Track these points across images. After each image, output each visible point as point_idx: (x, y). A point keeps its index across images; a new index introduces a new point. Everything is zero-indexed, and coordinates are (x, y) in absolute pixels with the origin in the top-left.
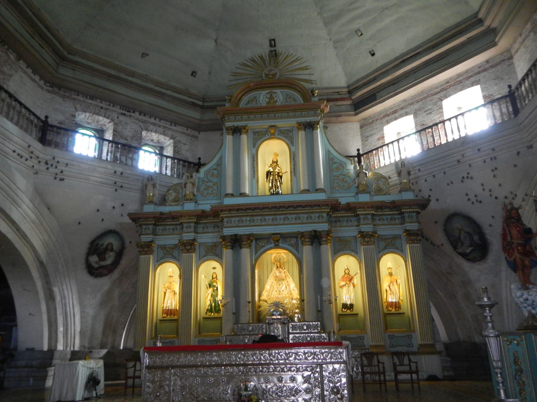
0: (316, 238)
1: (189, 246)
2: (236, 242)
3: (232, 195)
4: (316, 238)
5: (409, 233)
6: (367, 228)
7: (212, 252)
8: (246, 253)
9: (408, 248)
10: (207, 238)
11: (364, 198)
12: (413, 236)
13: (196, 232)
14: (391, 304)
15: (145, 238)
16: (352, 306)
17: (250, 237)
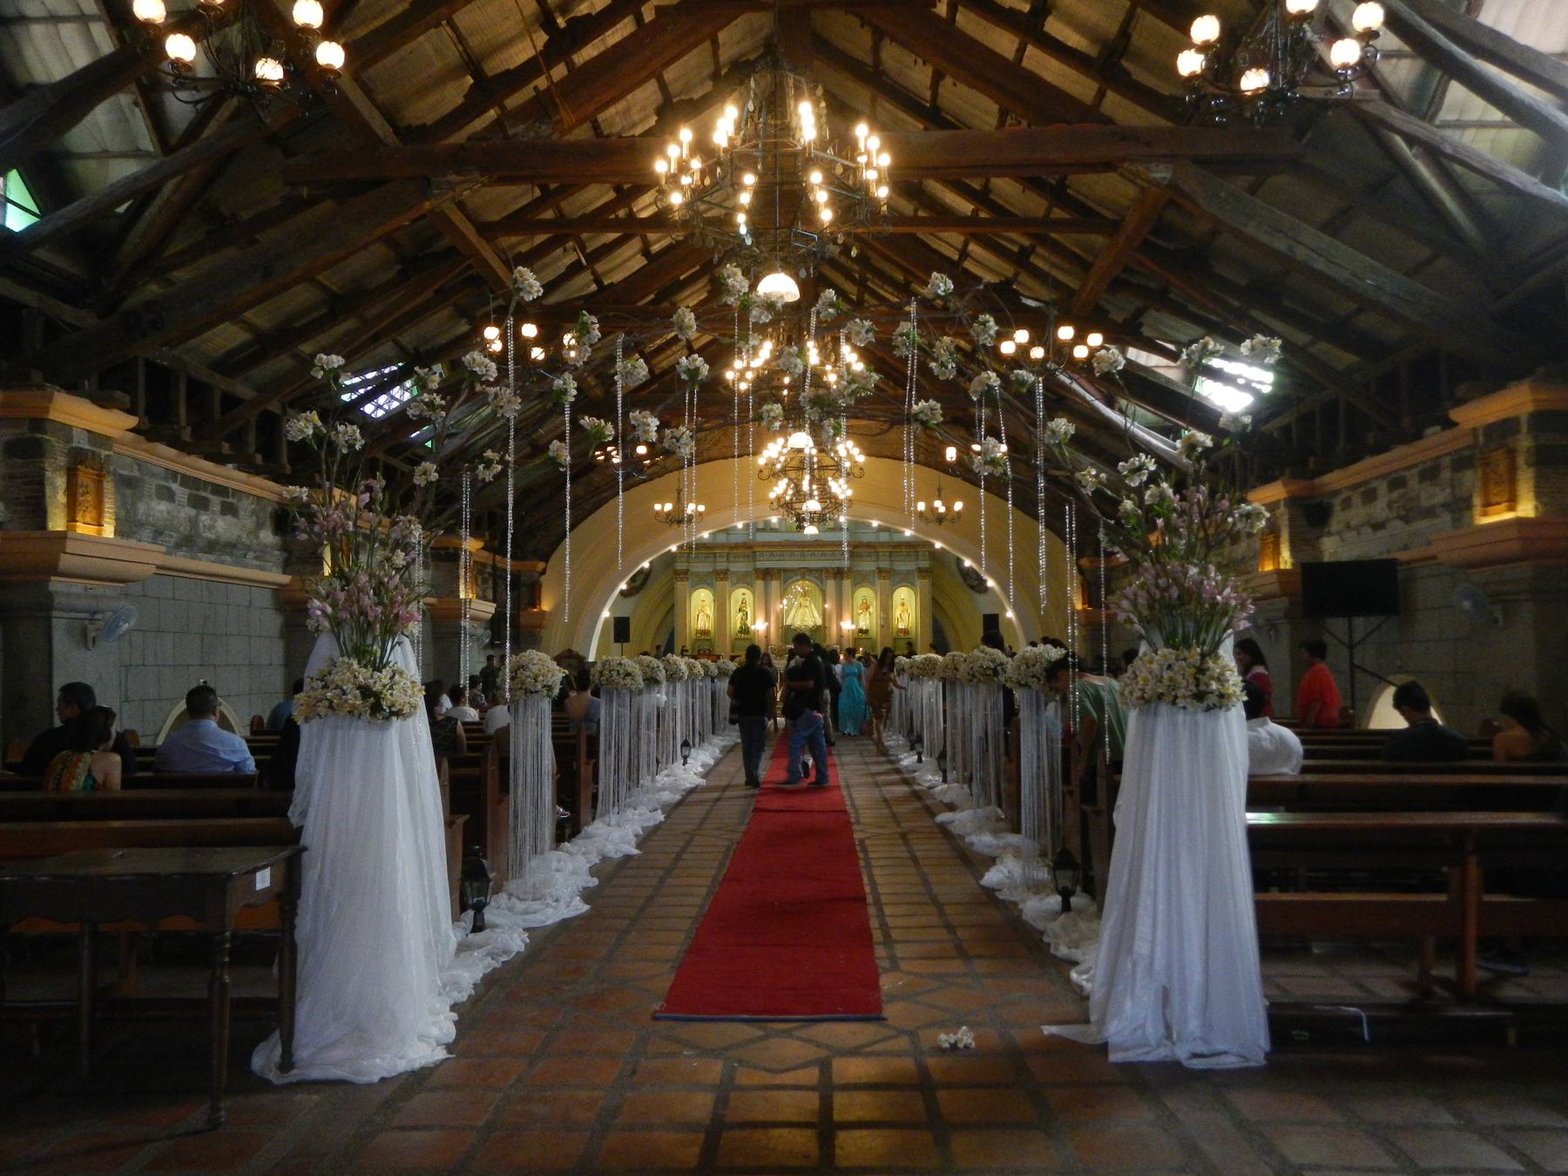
0: (839, 574)
1: (723, 575)
2: (766, 574)
3: (763, 530)
4: (839, 574)
5: (920, 570)
6: (885, 564)
7: (744, 580)
8: (775, 584)
9: (918, 583)
10: (739, 567)
11: (884, 537)
12: (922, 572)
13: (728, 561)
14: (901, 631)
15: (681, 566)
16: (866, 631)
17: (781, 571)
